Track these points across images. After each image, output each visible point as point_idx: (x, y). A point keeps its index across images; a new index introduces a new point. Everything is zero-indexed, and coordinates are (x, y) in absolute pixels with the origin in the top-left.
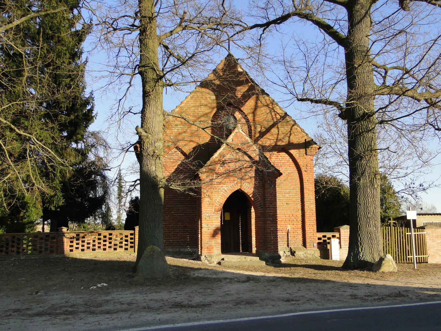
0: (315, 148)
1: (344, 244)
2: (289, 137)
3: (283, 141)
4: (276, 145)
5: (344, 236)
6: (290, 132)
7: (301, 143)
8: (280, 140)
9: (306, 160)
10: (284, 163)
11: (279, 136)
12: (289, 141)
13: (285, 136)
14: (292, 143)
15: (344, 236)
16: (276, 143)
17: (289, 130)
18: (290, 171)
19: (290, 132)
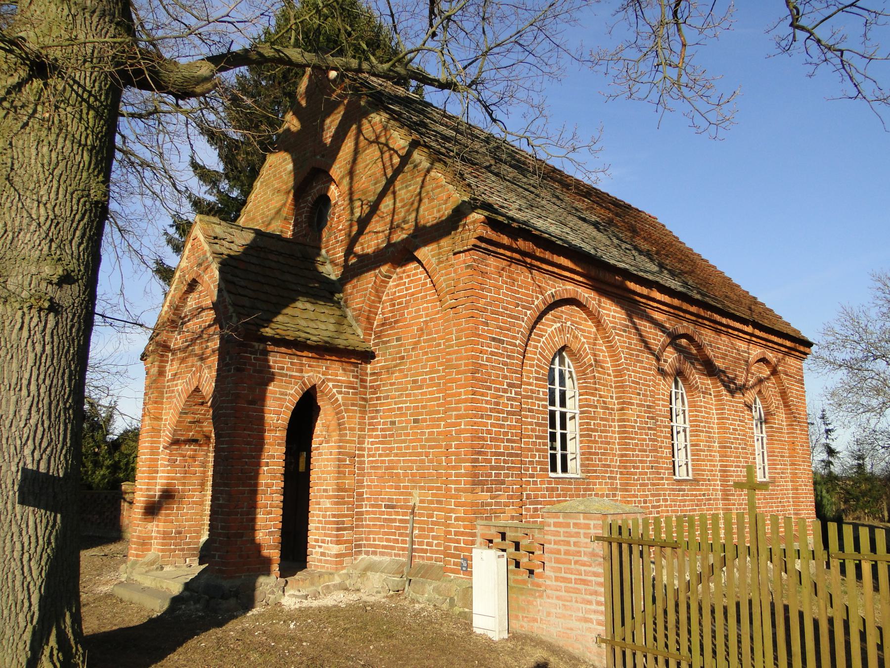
0: (474, 222)
1: (552, 574)
2: (417, 210)
3: (403, 229)
4: (389, 245)
5: (556, 543)
6: (420, 193)
7: (444, 218)
8: (398, 226)
9: (455, 271)
10: (412, 294)
11: (396, 217)
12: (417, 224)
13: (408, 210)
14: (424, 227)
15: (556, 543)
16: (389, 240)
17: (418, 190)
18: (427, 315)
19: (420, 193)
